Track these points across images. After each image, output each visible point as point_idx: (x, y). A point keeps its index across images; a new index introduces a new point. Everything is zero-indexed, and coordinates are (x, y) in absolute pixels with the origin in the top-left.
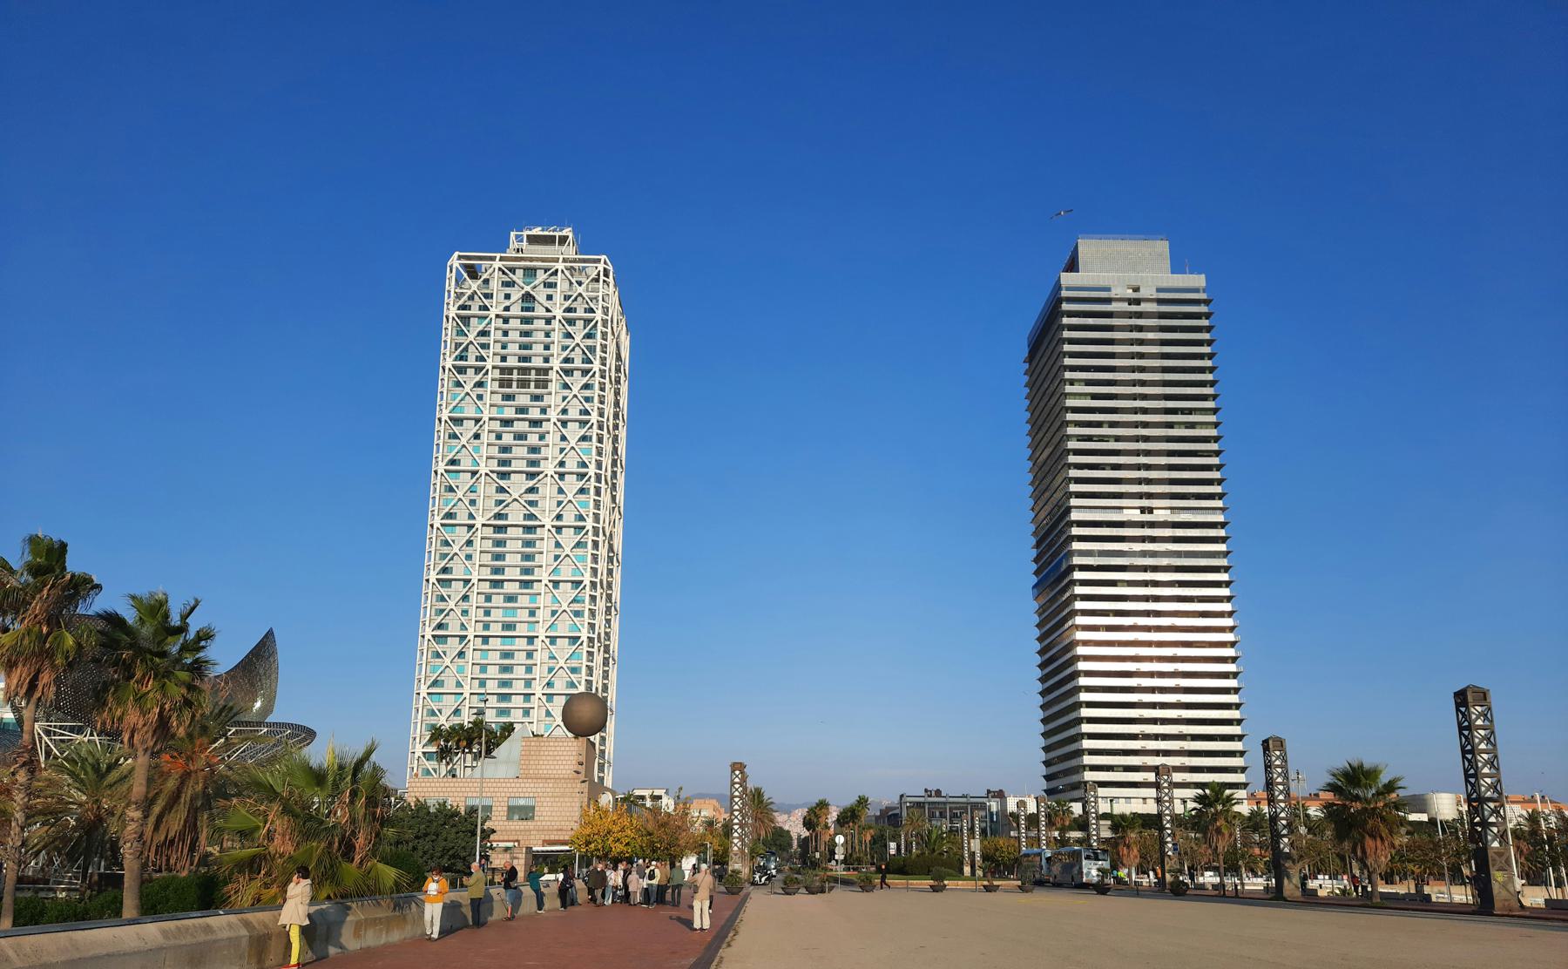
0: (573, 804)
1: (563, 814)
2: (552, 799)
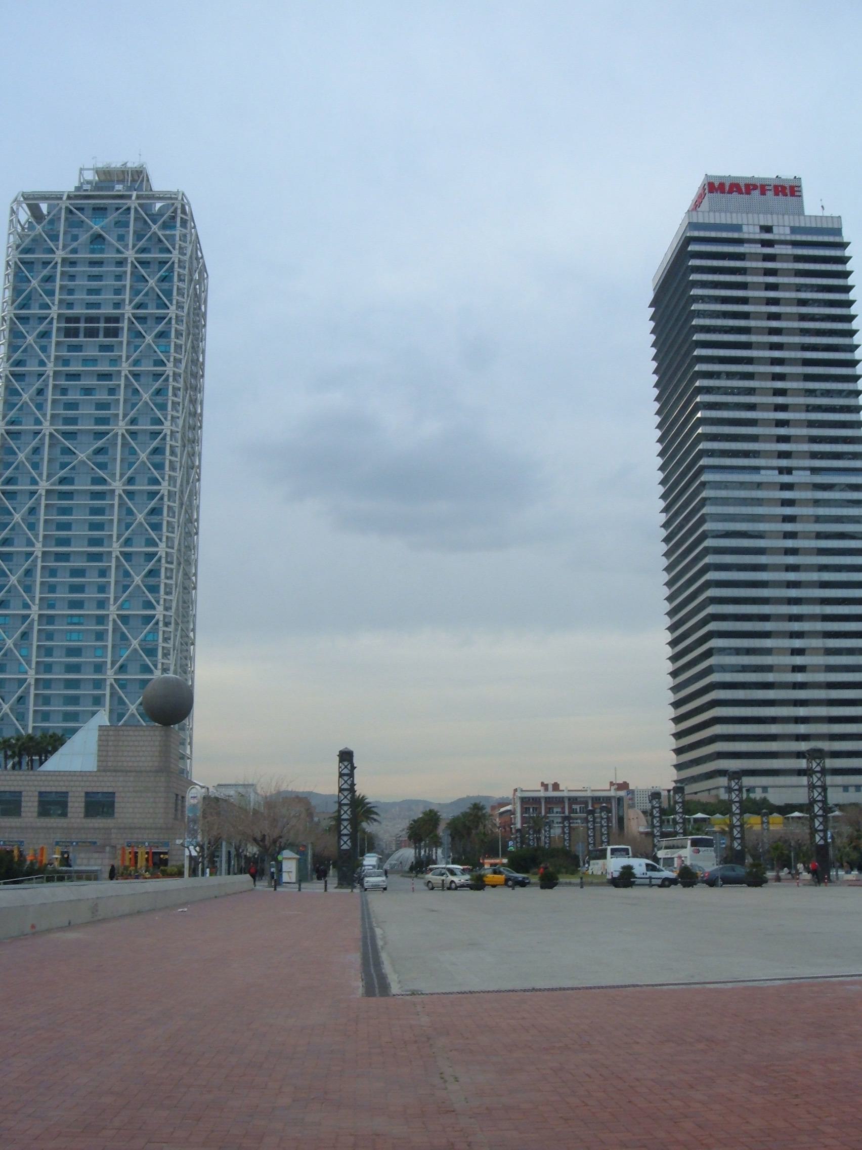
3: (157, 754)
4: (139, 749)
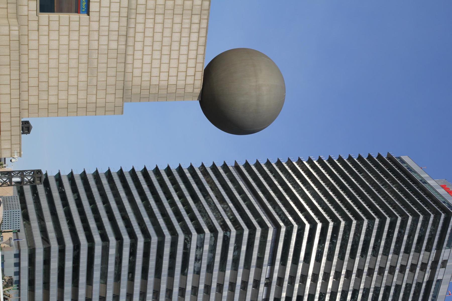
0: (73, 91)
1: (53, 73)
2: (84, 49)
3: (155, 81)
4: (166, 50)
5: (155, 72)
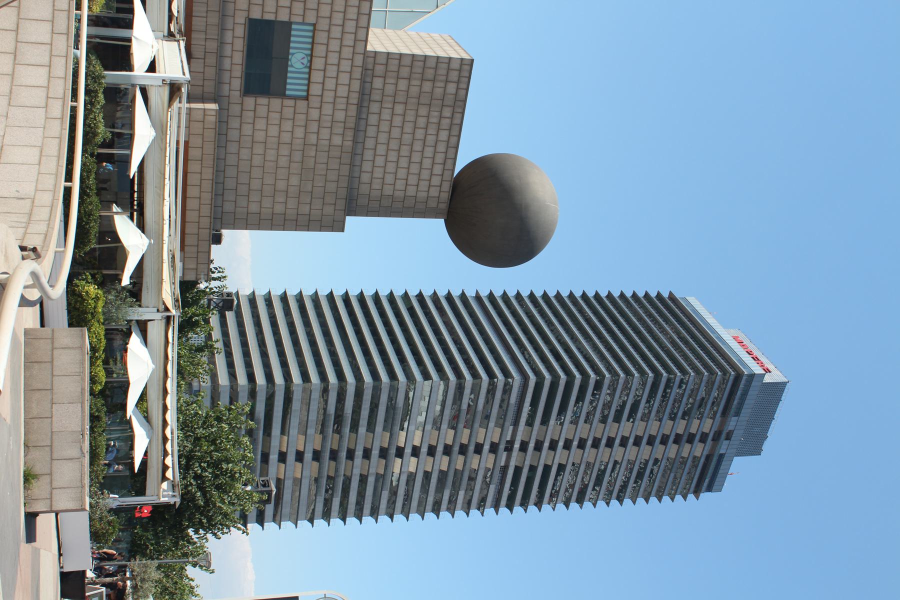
0: (280, 198)
1: (257, 173)
2: (298, 143)
3: (388, 190)
4: (405, 151)
5: (389, 179)
